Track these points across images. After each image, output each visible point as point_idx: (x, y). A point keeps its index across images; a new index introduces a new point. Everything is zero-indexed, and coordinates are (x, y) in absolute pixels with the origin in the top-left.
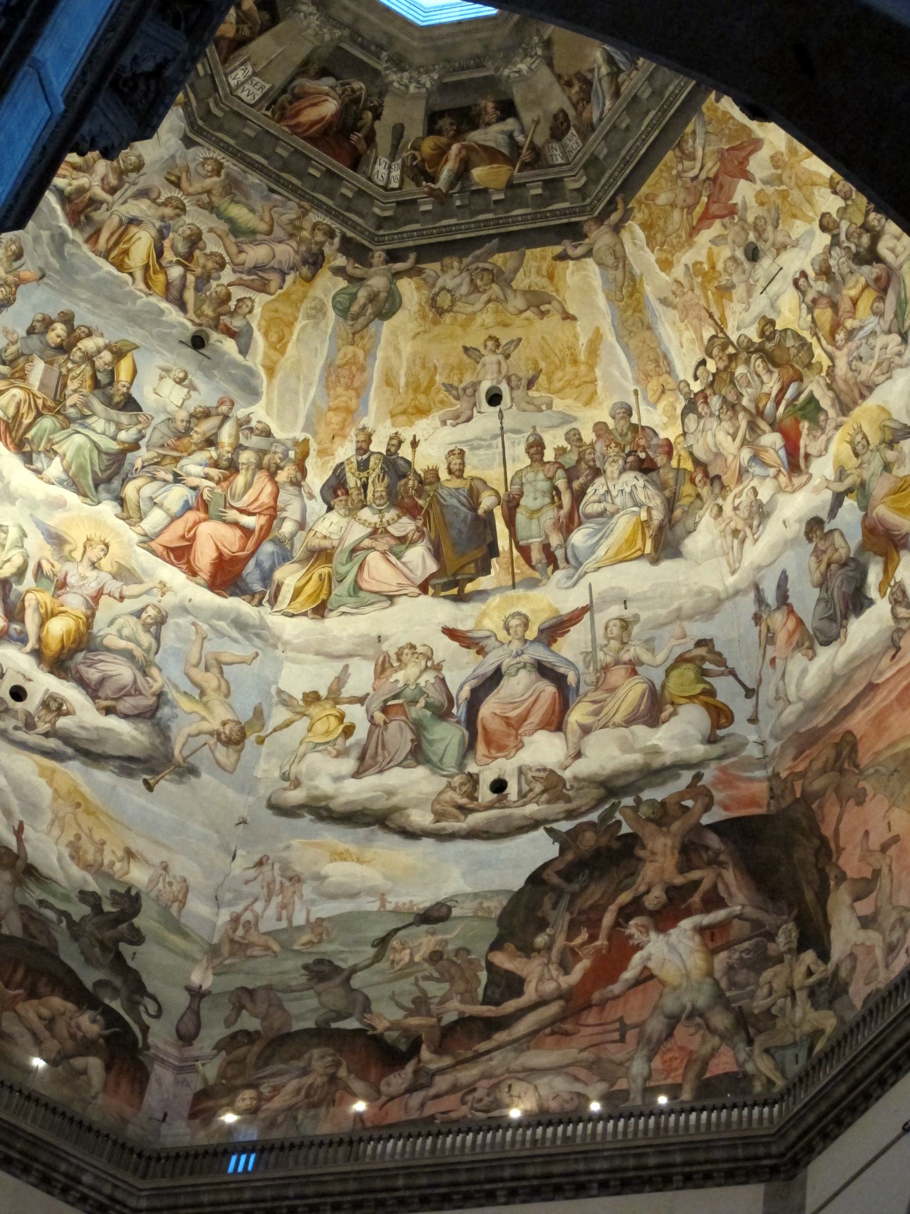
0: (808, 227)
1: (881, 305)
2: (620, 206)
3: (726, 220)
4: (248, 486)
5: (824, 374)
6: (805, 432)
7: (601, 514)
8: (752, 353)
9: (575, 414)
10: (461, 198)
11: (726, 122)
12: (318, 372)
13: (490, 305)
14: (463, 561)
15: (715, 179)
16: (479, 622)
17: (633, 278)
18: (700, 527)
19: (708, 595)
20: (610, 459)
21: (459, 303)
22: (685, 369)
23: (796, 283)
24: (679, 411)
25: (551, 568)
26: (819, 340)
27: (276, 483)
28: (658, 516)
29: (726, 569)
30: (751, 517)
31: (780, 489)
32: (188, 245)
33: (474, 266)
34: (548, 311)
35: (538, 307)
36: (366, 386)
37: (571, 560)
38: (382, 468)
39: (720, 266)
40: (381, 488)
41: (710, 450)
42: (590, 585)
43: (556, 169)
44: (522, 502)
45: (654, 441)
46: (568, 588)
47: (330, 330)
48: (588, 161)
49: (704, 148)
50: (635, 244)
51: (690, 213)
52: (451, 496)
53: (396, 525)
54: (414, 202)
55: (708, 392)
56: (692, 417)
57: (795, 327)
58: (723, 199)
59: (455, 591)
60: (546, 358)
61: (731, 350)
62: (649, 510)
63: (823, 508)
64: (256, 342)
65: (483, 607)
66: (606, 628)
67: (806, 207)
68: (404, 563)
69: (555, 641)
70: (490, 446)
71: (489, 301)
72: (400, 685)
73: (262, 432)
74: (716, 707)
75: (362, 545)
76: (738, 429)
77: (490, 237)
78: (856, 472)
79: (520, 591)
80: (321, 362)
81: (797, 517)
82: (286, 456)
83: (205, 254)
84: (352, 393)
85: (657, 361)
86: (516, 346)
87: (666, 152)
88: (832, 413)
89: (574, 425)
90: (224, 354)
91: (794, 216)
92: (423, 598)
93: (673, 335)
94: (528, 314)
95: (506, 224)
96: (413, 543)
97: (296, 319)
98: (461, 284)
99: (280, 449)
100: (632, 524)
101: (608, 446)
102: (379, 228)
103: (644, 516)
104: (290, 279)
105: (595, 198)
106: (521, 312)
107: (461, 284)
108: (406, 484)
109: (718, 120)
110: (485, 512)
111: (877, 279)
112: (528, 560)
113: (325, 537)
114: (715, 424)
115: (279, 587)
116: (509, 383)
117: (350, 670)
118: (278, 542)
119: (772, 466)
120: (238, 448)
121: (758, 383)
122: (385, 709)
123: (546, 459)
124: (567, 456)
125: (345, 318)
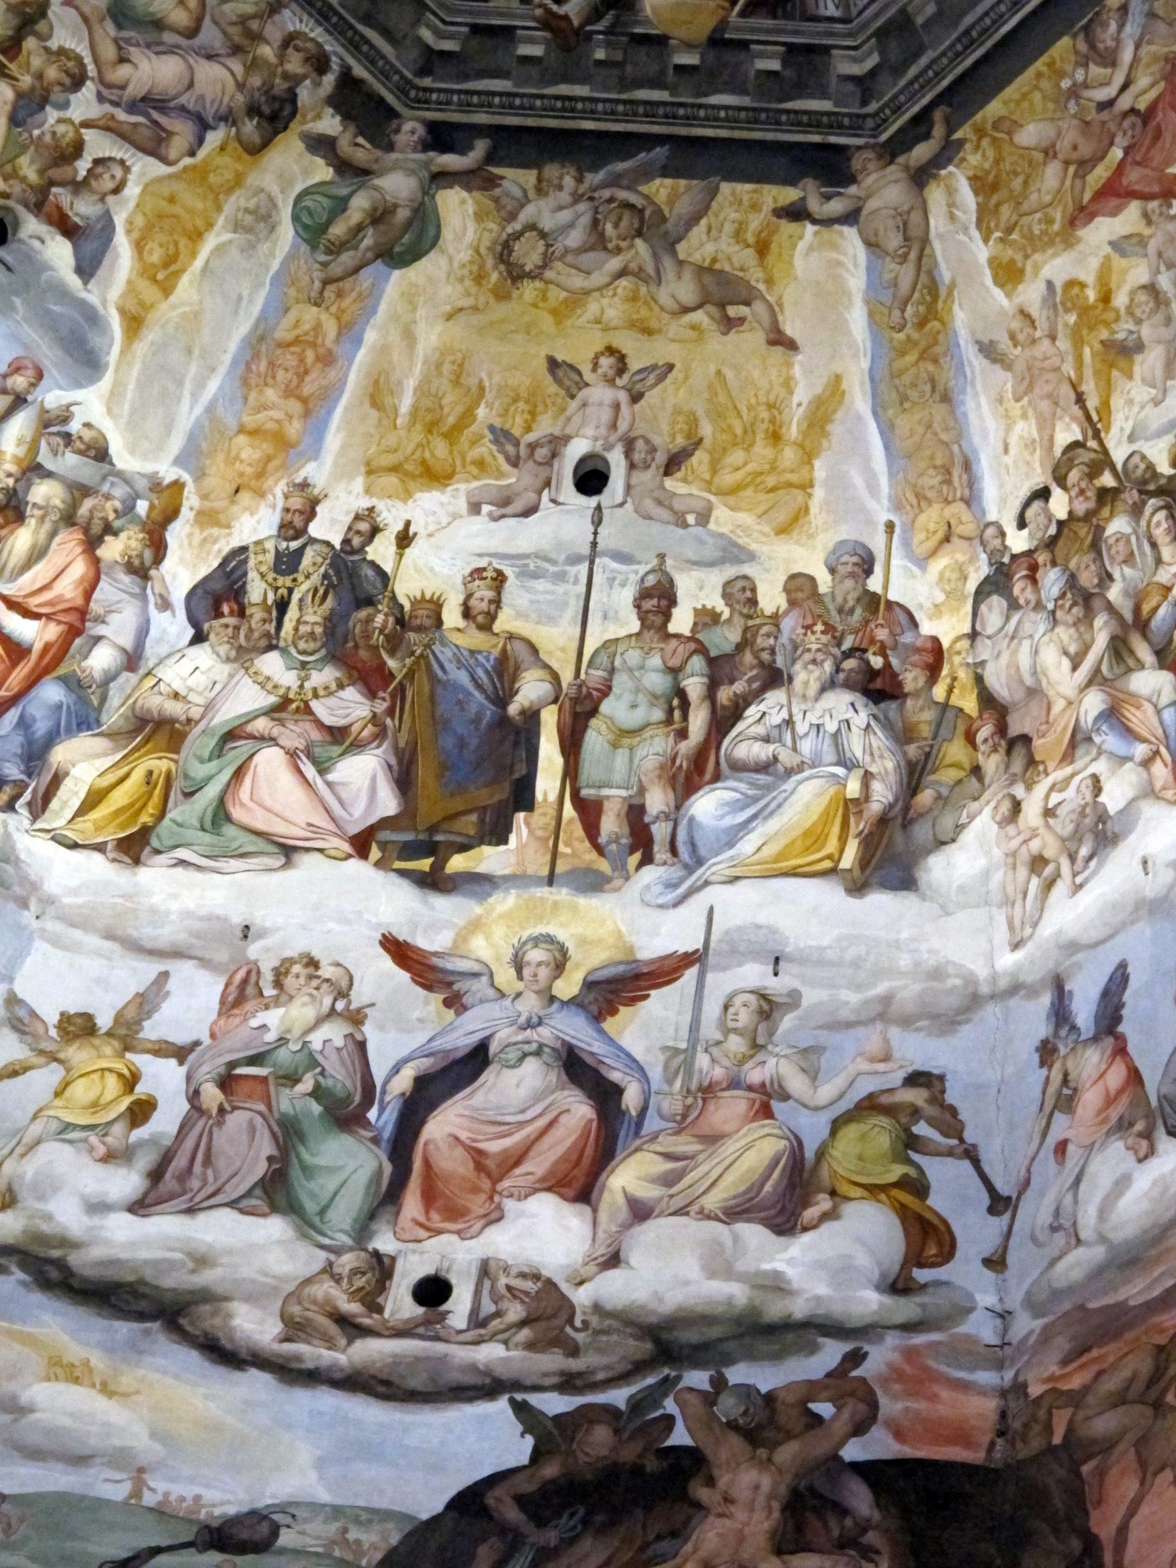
2: (938, 131)
3: (1153, 205)
4: (37, 554)
7: (766, 767)
8: (1152, 494)
9: (754, 547)
10: (608, 45)
12: (233, 346)
13: (624, 282)
14: (457, 805)
15: (1146, 117)
16: (462, 937)
17: (933, 288)
20: (808, 657)
21: (558, 265)
22: (1003, 500)
24: (972, 586)
25: (636, 857)
27: (96, 562)
28: (882, 794)
29: (1002, 934)
30: (1077, 836)
31: (1150, 792)
32: (15, 22)
33: (606, 193)
34: (742, 320)
35: (722, 306)
36: (330, 395)
37: (682, 849)
38: (325, 576)
39: (1120, 300)
40: (314, 617)
41: (1021, 681)
42: (711, 911)
43: (821, 27)
44: (605, 707)
45: (907, 638)
46: (661, 906)
47: (275, 265)
48: (890, 22)
49: (1137, 46)
50: (952, 217)
51: (1081, 175)
52: (460, 665)
53: (332, 701)
54: (507, 33)
55: (1042, 558)
56: (995, 605)
58: (1157, 157)
59: (425, 864)
60: (717, 415)
62: (867, 777)
64: (117, 256)
65: (478, 910)
66: (726, 1008)
68: (329, 785)
69: (613, 1012)
70: (561, 577)
71: (622, 273)
72: (270, 1037)
73: (89, 447)
74: (920, 1219)
75: (249, 728)
77: (649, 141)
79: (561, 894)
80: (243, 328)
82: (128, 509)
83: (46, 49)
84: (295, 406)
86: (661, 379)
87: (1060, 36)
89: (747, 569)
90: (46, 267)
92: (355, 865)
94: (699, 316)
95: (690, 120)
96: (358, 746)
97: (210, 225)
98: (571, 225)
99: (120, 491)
100: (824, 801)
101: (808, 627)
102: (423, 72)
103: (853, 788)
104: (213, 139)
105: (886, 105)
106: (686, 310)
107: (571, 225)
108: (369, 620)
110: (523, 712)
112: (591, 828)
113: (176, 696)
114: (1042, 628)
115: (57, 780)
116: (628, 453)
117: (171, 985)
118: (74, 684)
119: (1144, 740)
120: (33, 470)
121: (1150, 559)
122: (227, 1082)
123: (672, 628)
124: (718, 629)
125: (314, 247)
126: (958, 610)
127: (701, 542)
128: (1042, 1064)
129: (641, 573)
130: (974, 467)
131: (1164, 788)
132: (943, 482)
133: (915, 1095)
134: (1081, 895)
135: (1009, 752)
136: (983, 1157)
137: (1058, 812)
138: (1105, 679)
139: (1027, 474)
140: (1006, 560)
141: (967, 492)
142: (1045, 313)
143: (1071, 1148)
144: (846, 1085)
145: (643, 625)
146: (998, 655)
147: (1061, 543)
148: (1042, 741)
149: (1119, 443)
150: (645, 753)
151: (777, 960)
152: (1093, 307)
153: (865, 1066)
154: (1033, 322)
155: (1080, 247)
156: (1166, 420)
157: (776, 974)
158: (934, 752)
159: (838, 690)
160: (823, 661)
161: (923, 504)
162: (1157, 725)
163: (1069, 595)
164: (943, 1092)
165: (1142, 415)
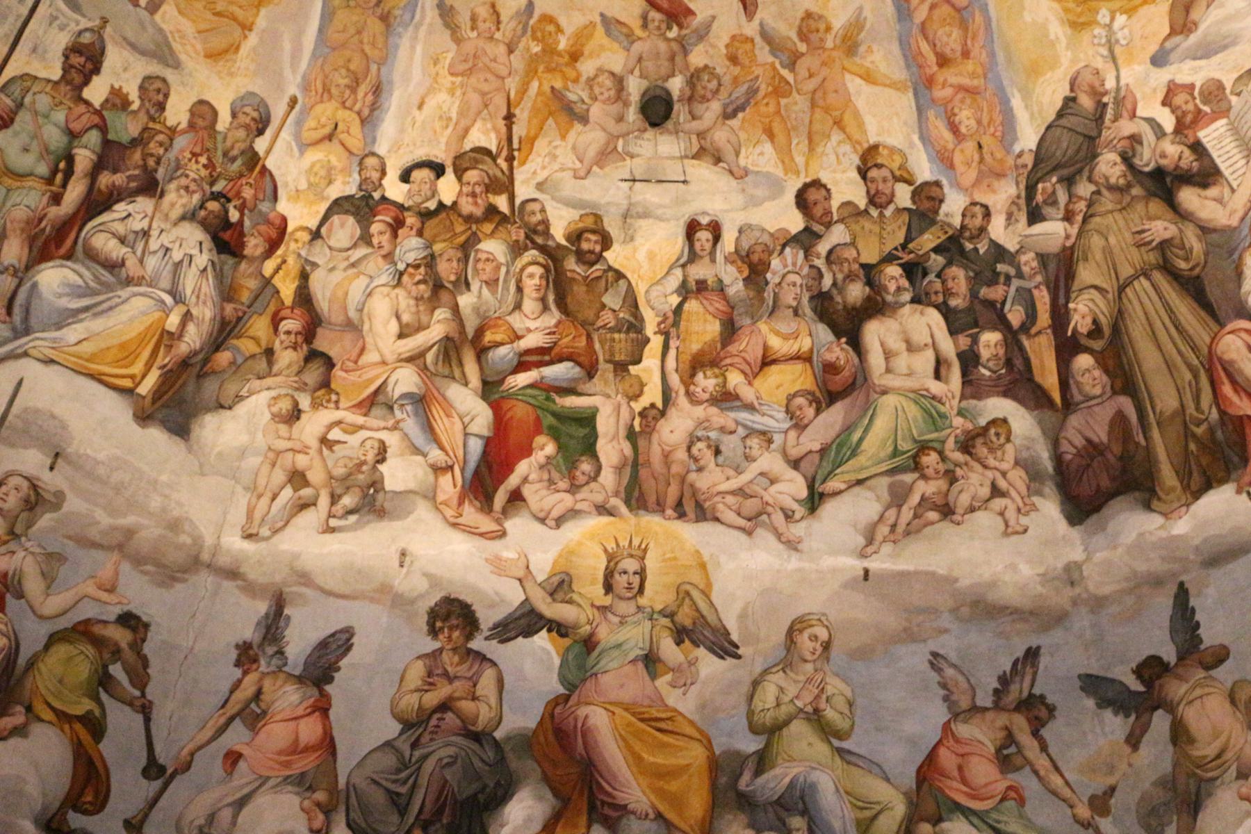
0: (779, 172)
1: (810, 412)
3: (655, 15)
5: (638, 406)
6: (539, 456)
7: (114, 266)
9: (183, 57)
18: (242, 409)
19: (184, 539)
20: (183, 181)
22: (396, 147)
23: (692, 228)
24: (335, 192)
26: (666, 347)
28: (193, 338)
29: (238, 515)
30: (346, 482)
31: (431, 496)
37: (17, 310)
39: (587, 67)
41: (345, 309)
42: (20, 383)
45: (264, 207)
55: (411, 220)
57: (640, 289)
61: (502, 203)
62: (187, 317)
63: (492, 606)
74: (91, 762)
76: (420, 328)
88: (608, 477)
89: (169, 74)
91: (770, 135)
93: (417, 73)
100: (148, 321)
114: (384, 279)
119: (442, 448)
123: (87, 93)
124: (123, 116)
126: (311, 203)
127: (144, 28)
128: (238, 664)
129: (81, 27)
130: (384, 95)
131: (445, 503)
132: (347, 86)
133: (121, 636)
134: (328, 536)
135: (308, 359)
136: (154, 716)
137: (335, 448)
138: (426, 368)
139: (430, 141)
140: (376, 195)
141: (366, 112)
142: (513, 24)
143: (242, 765)
144: (71, 603)
145: (63, 77)
146: (332, 269)
148: (343, 374)
149: (524, 182)
150: (18, 200)
151: (57, 455)
152: (559, 54)
153: (90, 589)
154: (499, 22)
156: (578, 196)
157: (52, 468)
158: (246, 318)
159: (195, 225)
160: (194, 192)
161: (326, 95)
162: (460, 444)
163: (422, 270)
164: (144, 640)
165: (559, 175)
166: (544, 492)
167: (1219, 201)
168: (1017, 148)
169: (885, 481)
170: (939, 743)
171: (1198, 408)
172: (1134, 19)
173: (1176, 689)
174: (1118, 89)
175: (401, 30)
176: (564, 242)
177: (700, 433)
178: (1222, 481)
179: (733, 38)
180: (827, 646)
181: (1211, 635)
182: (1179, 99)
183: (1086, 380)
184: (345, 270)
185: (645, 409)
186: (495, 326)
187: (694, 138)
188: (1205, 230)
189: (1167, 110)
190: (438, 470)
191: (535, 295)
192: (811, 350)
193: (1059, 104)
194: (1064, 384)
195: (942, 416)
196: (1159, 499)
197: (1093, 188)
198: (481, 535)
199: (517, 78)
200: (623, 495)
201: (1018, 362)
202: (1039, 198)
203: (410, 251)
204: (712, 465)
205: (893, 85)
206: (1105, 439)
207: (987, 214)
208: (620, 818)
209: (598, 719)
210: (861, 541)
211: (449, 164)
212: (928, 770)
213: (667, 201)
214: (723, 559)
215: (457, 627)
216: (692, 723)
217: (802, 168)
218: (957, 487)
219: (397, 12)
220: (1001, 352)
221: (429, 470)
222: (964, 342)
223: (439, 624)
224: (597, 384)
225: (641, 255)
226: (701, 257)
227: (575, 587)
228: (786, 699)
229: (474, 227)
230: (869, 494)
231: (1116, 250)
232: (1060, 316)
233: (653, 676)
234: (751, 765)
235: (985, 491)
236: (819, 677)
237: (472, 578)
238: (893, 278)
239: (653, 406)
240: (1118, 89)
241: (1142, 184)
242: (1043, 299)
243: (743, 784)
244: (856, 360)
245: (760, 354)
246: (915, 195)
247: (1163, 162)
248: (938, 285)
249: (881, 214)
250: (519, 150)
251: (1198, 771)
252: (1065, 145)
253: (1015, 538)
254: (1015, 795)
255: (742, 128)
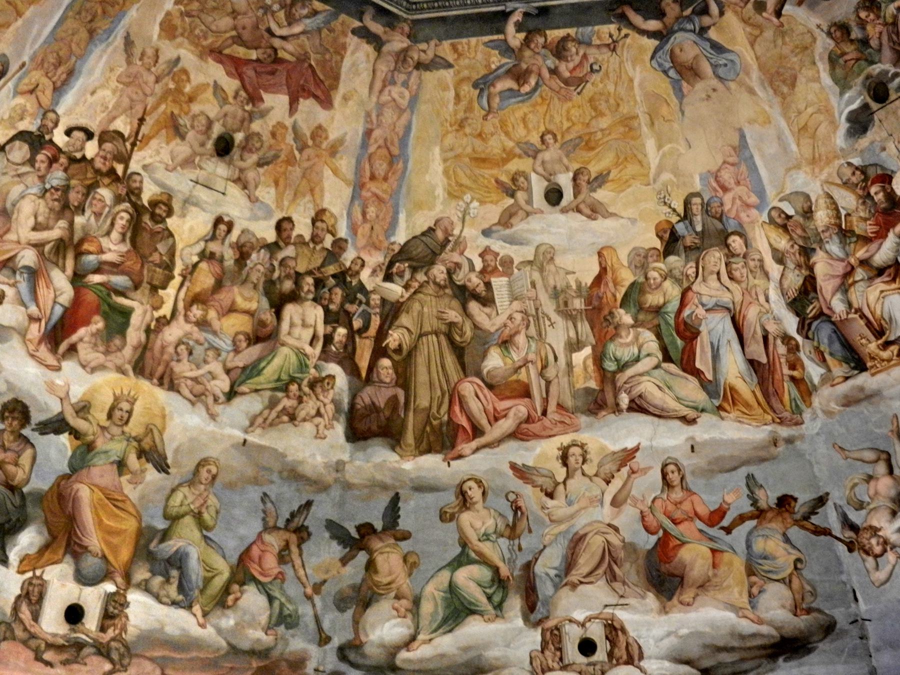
0: (273, 206)
1: (244, 344)
3: (243, 93)
5: (156, 314)
8: (130, 201)
11: (337, 53)
15: (277, 61)
22: (69, 112)
23: (218, 221)
24: (23, 126)
26: (182, 285)
31: (23, 334)
39: (196, 108)
41: (5, 201)
49: (304, 32)
55: (63, 160)
57: (180, 246)
61: (120, 169)
63: (41, 410)
67: (289, 195)
76: (47, 228)
78: (96, 428)
81: (11, 379)
85: (59, 63)
88: (128, 352)
91: (276, 183)
93: (98, 72)
109: (335, 40)
111: (262, 324)
114: (35, 190)
119: (38, 306)
130: (73, 79)
131: (30, 340)
132: (53, 64)
139: (91, 117)
140: (47, 137)
141: (59, 84)
142: (164, 67)
147: (76, 166)
152: (183, 94)
154: (157, 62)
155: (203, 64)
162: (50, 308)
163: (59, 193)
165: (158, 165)
166: (90, 350)
167: (489, 316)
168: (393, 239)
169: (268, 394)
170: (254, 542)
171: (438, 412)
172: (482, 207)
173: (376, 544)
174: (459, 236)
175: (98, 42)
176: (146, 204)
177: (185, 340)
178: (437, 452)
179: (278, 123)
180: (214, 477)
181: (404, 523)
182: (489, 257)
183: (383, 372)
184: (13, 177)
185: (160, 317)
186: (92, 241)
187: (237, 172)
188: (476, 327)
189: (480, 259)
190: (32, 319)
191: (120, 230)
192: (255, 311)
193: (425, 228)
194: (370, 369)
195: (307, 366)
196: (401, 447)
197: (426, 279)
198: (47, 366)
199: (154, 100)
200: (133, 364)
201: (350, 348)
202: (394, 270)
203: (56, 178)
204: (185, 361)
205: (345, 180)
206: (382, 406)
207: (363, 266)
208: (82, 554)
209: (84, 493)
210: (247, 423)
211: (97, 134)
212: (245, 556)
213: (210, 200)
214: (176, 415)
215: (17, 418)
216: (134, 506)
217: (285, 208)
218: (302, 406)
219: (100, 31)
220: (344, 340)
221: (27, 318)
222: (329, 329)
223: (7, 414)
224: (138, 294)
225: (186, 227)
226: (217, 239)
227: (91, 411)
228: (187, 503)
229: (99, 178)
230: (259, 399)
231: (426, 316)
232: (382, 334)
233: (120, 474)
234: (159, 536)
235: (313, 412)
236: (205, 494)
237: (34, 391)
238: (308, 284)
239: (165, 317)
240: (459, 236)
241: (452, 290)
242: (376, 322)
243: (152, 546)
244: (275, 323)
245: (229, 303)
246: (334, 243)
247: (468, 284)
248: (327, 296)
249: (314, 248)
250: (141, 141)
251: (375, 589)
252: (419, 250)
253: (319, 441)
254: (281, 577)
255: (264, 174)
